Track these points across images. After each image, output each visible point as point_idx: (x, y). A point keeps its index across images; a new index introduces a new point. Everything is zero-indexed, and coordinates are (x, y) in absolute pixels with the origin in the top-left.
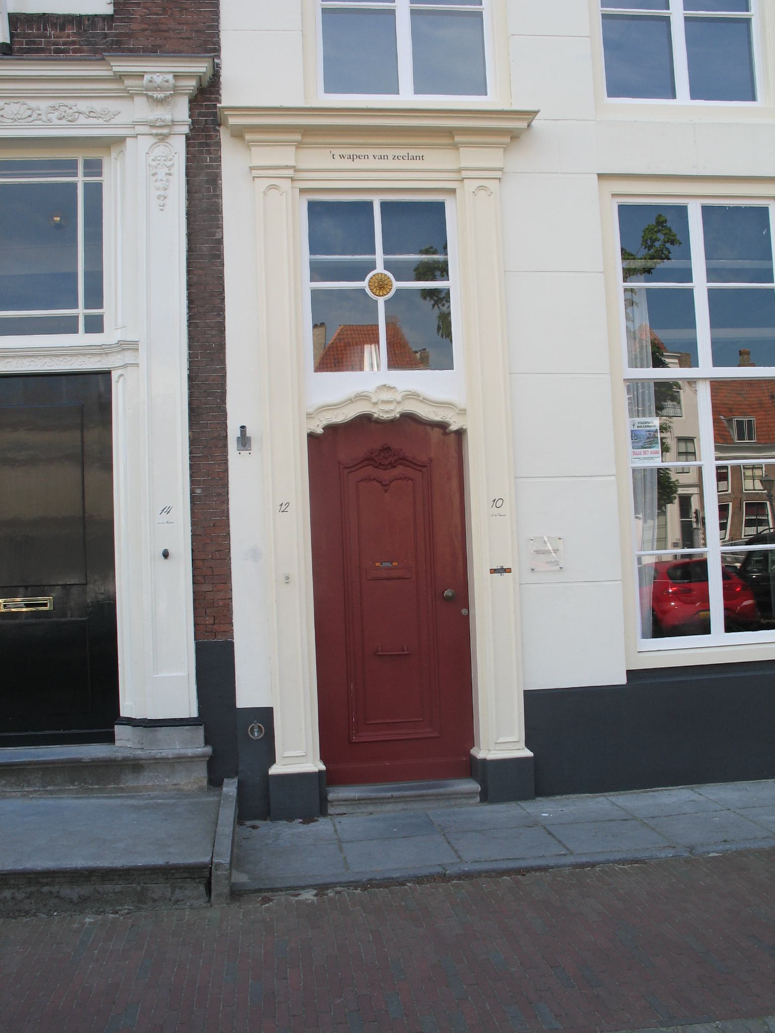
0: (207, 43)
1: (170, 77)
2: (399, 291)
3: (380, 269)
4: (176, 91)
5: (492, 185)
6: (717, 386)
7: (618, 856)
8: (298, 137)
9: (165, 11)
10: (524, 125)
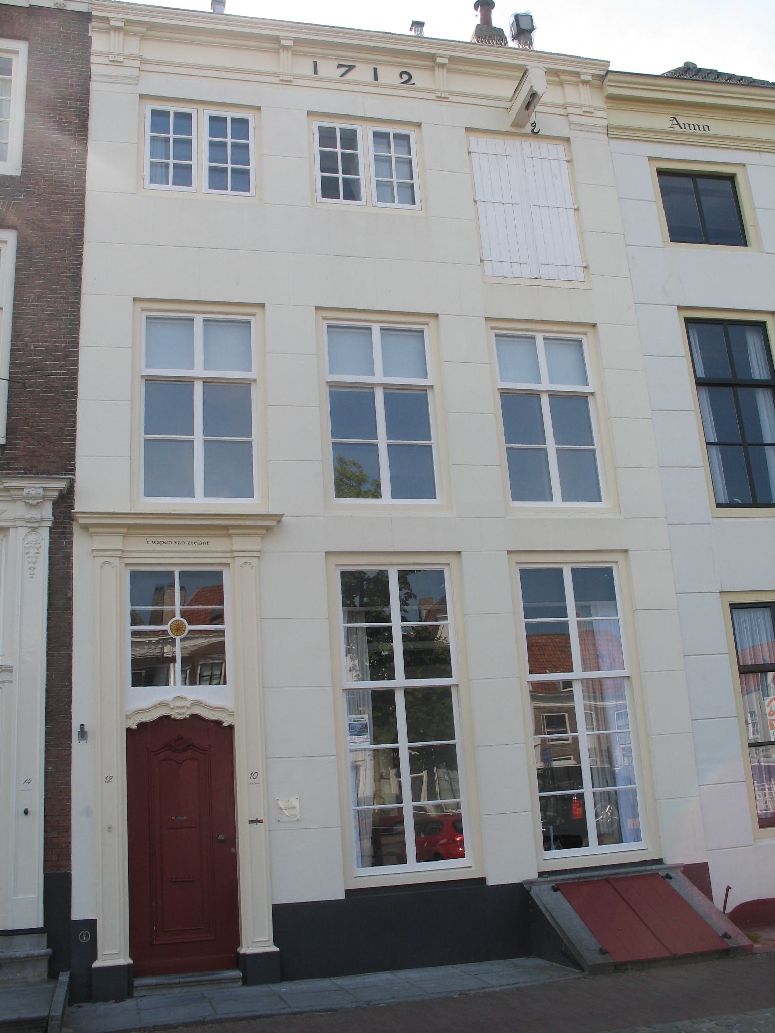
0: (64, 464)
1: (41, 491)
2: (190, 632)
3: (178, 617)
4: (44, 498)
5: (254, 561)
6: (408, 692)
7: (318, 1008)
8: (124, 530)
9: (39, 444)
10: (274, 523)
